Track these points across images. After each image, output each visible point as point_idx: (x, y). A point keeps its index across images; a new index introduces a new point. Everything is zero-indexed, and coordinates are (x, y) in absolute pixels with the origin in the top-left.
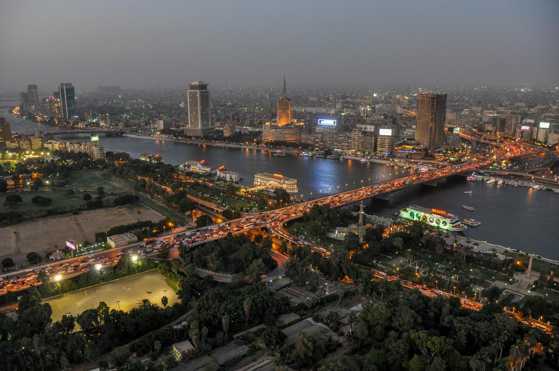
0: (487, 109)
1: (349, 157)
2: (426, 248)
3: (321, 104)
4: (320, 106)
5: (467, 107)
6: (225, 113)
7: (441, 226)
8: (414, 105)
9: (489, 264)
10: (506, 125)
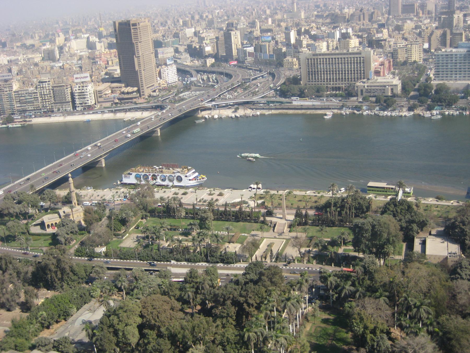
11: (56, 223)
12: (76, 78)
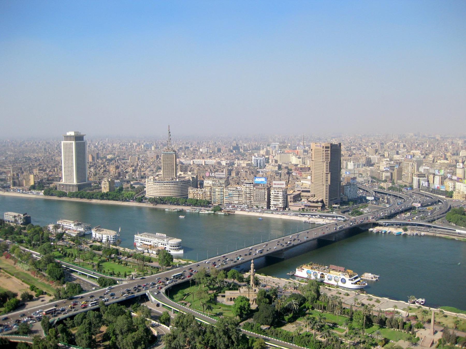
10: (403, 173)
11: (234, 298)
12: (275, 184)
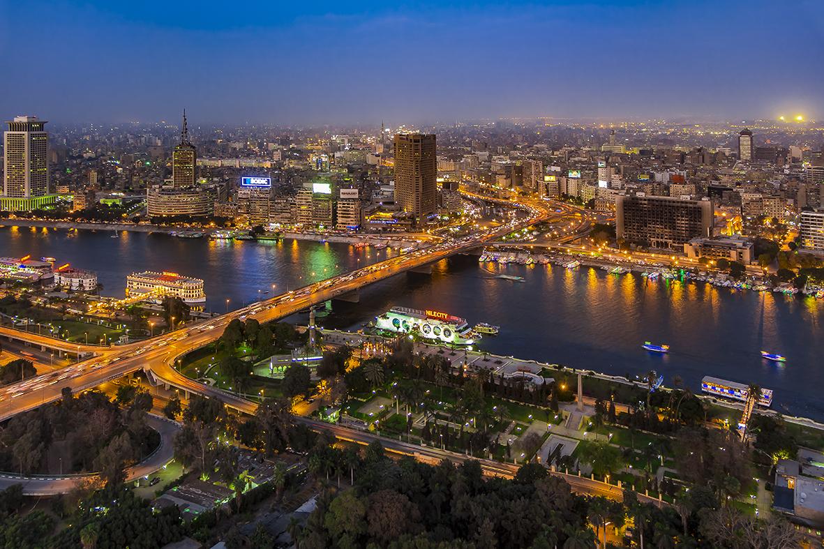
0: (497, 154)
1: (293, 236)
2: (421, 376)
3: (249, 154)
4: (248, 156)
5: (469, 153)
6: (79, 171)
7: (442, 337)
8: (391, 152)
9: (518, 396)
